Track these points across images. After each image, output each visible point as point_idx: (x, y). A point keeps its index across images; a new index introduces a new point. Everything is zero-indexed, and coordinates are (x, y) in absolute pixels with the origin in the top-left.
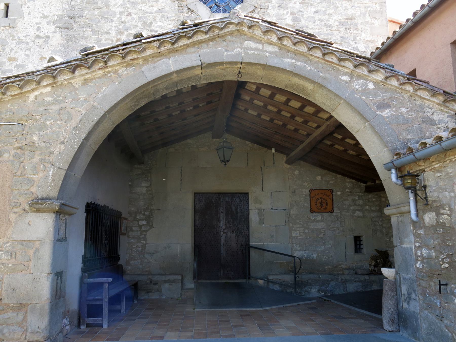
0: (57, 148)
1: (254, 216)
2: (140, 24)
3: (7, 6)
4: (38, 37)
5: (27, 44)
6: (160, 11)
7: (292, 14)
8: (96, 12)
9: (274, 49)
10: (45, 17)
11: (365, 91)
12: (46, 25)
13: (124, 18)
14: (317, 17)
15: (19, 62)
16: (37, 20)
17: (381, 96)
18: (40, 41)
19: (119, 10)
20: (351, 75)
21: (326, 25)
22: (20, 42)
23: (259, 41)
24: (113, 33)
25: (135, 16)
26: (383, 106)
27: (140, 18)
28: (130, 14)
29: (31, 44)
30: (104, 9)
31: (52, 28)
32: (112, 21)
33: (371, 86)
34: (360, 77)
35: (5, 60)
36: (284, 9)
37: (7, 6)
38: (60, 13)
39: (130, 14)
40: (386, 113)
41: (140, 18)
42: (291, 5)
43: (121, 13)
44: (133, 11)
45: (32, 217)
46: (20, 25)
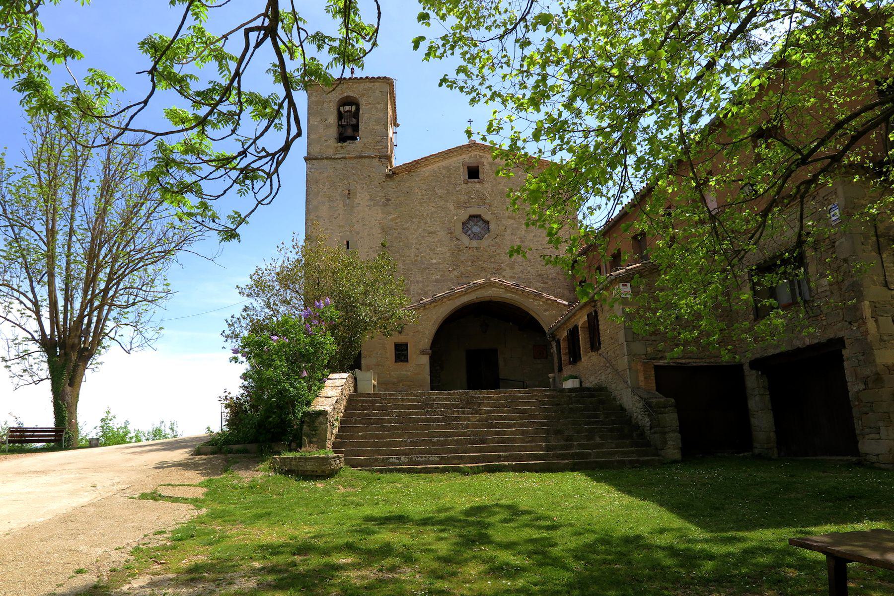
0: (427, 332)
1: (501, 362)
6: (439, 241)
7: (520, 238)
8: (401, 243)
9: (504, 290)
10: (371, 248)
11: (539, 305)
13: (418, 247)
14: (535, 239)
16: (366, 250)
17: (545, 307)
20: (533, 299)
21: (541, 244)
23: (498, 288)
24: (412, 256)
26: (546, 310)
27: (427, 246)
30: (406, 241)
33: (541, 303)
34: (537, 300)
36: (515, 235)
37: (348, 242)
40: (547, 313)
41: (427, 246)
42: (519, 232)
43: (416, 243)
45: (421, 356)
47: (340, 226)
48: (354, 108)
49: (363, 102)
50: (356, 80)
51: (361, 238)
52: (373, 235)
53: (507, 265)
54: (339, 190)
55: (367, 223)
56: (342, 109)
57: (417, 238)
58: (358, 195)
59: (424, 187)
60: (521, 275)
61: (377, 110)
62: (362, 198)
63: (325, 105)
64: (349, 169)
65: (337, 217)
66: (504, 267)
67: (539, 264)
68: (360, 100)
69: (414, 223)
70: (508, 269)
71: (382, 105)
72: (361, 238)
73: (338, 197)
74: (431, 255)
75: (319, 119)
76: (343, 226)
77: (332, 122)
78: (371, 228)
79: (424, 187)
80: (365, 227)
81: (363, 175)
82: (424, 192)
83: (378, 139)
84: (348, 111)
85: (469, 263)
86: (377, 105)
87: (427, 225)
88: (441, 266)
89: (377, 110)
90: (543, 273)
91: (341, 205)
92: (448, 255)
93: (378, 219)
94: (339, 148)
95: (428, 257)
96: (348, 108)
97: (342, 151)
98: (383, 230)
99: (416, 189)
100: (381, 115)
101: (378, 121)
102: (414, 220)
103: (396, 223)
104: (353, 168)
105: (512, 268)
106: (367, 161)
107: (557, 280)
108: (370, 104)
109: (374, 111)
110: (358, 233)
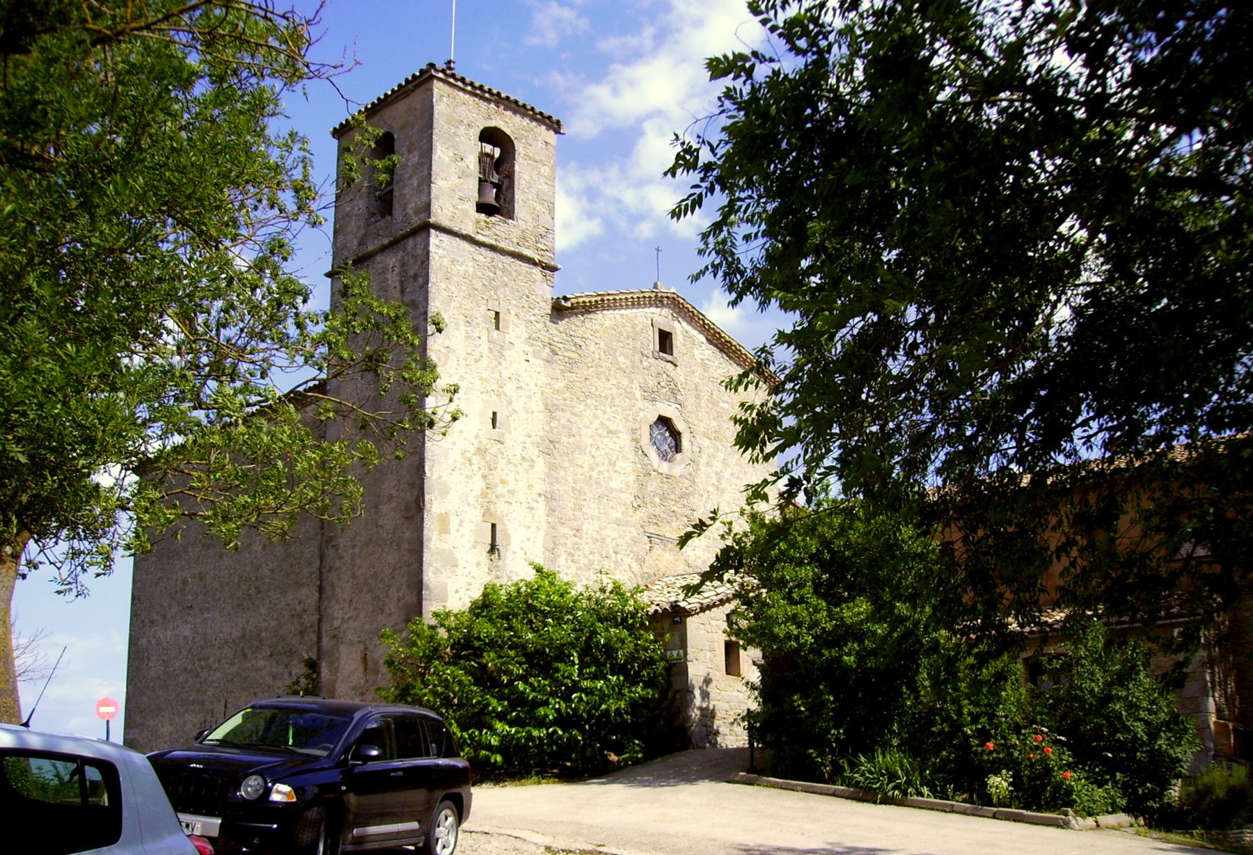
4: (523, 458)
5: (516, 466)
7: (717, 473)
12: (530, 447)
15: (511, 487)
16: (523, 438)
18: (526, 464)
19: (589, 441)
24: (586, 467)
28: (598, 448)
31: (536, 452)
32: (585, 454)
35: (497, 481)
37: (494, 414)
38: (541, 433)
39: (598, 448)
44: (600, 445)
46: (509, 439)
47: (481, 379)
50: (513, 106)
54: (483, 308)
55: (524, 386)
58: (511, 326)
61: (539, 173)
62: (515, 331)
64: (498, 272)
65: (476, 361)
71: (547, 168)
73: (480, 320)
74: (611, 472)
79: (602, 346)
80: (521, 392)
83: (542, 231)
85: (657, 500)
87: (606, 416)
88: (624, 496)
91: (485, 338)
92: (632, 478)
94: (482, 223)
95: (606, 475)
97: (486, 232)
98: (546, 405)
104: (504, 271)
106: (525, 267)
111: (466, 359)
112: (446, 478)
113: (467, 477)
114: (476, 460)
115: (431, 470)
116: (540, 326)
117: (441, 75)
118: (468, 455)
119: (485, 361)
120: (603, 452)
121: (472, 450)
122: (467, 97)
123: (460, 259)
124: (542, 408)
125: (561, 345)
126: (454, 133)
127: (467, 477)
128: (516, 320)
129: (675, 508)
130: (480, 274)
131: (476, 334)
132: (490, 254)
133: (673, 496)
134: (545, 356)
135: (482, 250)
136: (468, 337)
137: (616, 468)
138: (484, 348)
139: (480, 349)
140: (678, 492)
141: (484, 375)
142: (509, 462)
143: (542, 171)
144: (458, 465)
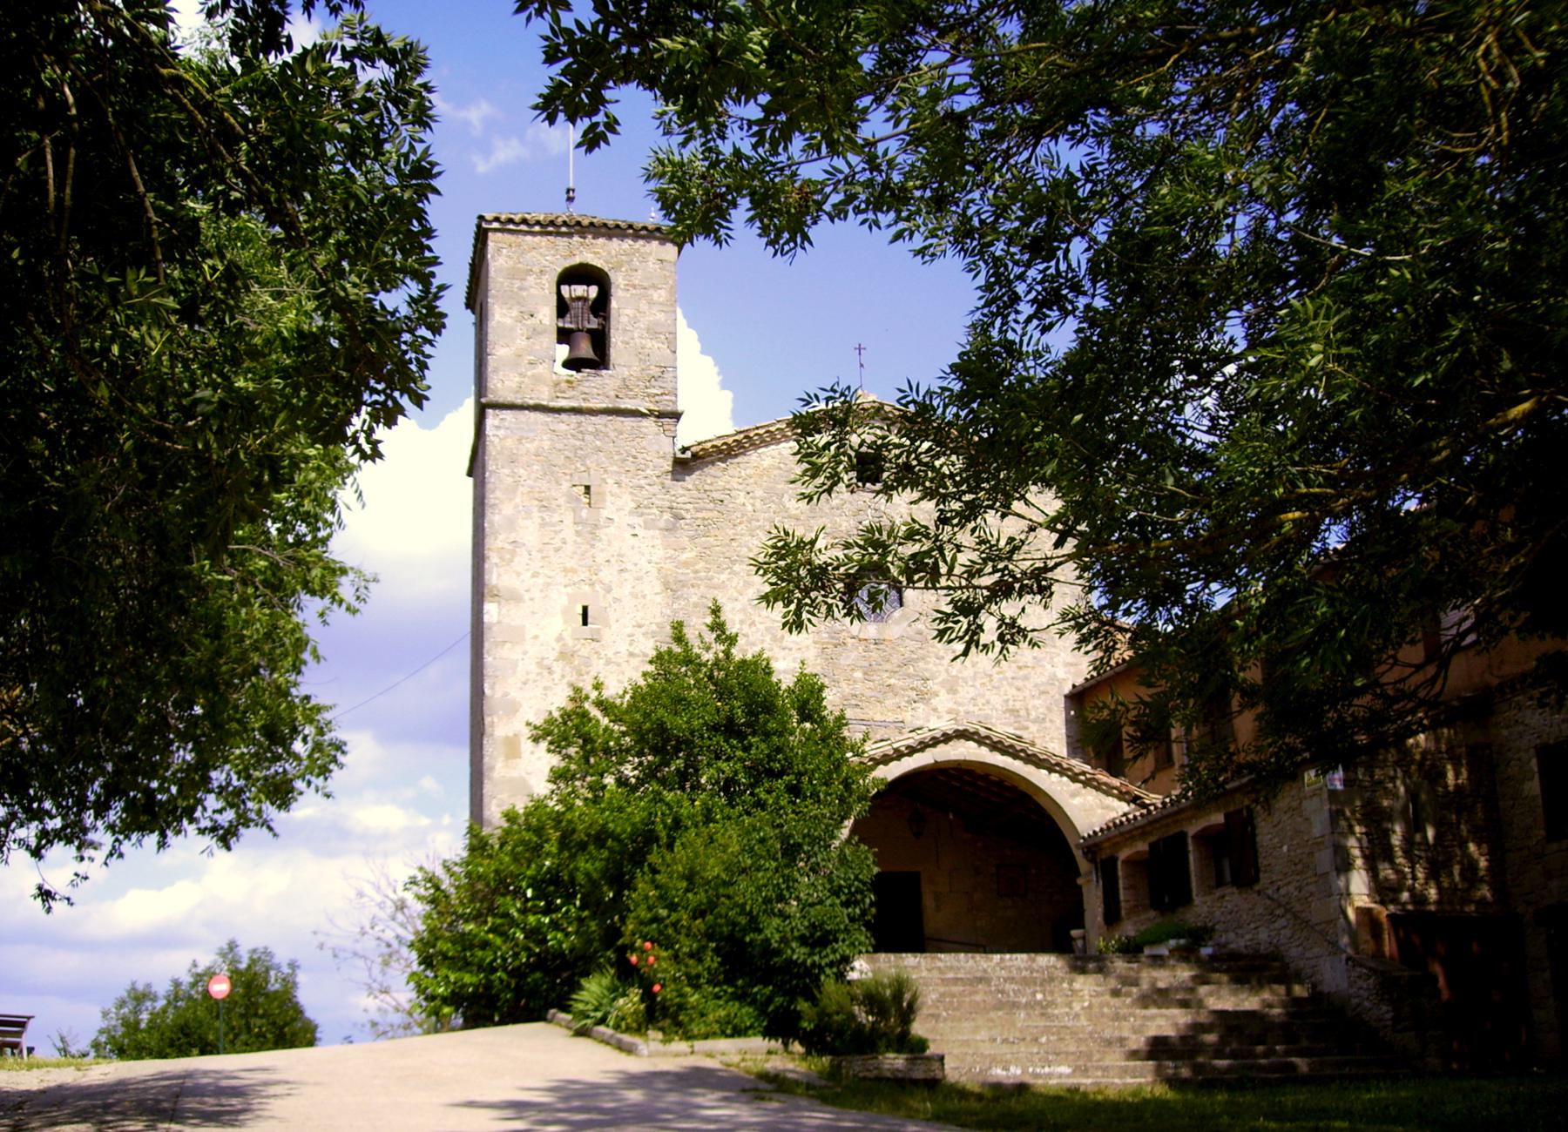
2: (768, 639)
3: (585, 609)
4: (631, 654)
5: (619, 665)
10: (640, 626)
12: (641, 638)
16: (629, 630)
22: (609, 662)
25: (762, 627)
26: (1074, 795)
28: (753, 624)
29: (624, 665)
37: (585, 609)
38: (659, 620)
39: (753, 624)
41: (767, 629)
43: (742, 622)
44: (757, 619)
46: (607, 635)
47: (565, 570)
48: (593, 292)
49: (618, 280)
51: (616, 600)
52: (644, 597)
53: (942, 684)
54: (566, 485)
55: (630, 566)
56: (565, 290)
57: (743, 610)
58: (609, 498)
59: (759, 493)
60: (971, 708)
61: (651, 303)
62: (617, 504)
63: (531, 279)
64: (587, 437)
65: (557, 550)
66: (936, 688)
67: (1011, 685)
68: (612, 275)
69: (736, 573)
70: (943, 693)
71: (663, 292)
72: (616, 600)
73: (562, 501)
75: (515, 313)
76: (573, 571)
77: (546, 321)
78: (639, 579)
79: (759, 493)
80: (625, 575)
81: (618, 453)
82: (758, 504)
83: (655, 371)
84: (579, 299)
85: (858, 674)
86: (651, 292)
89: (651, 303)
90: (1018, 705)
91: (569, 519)
93: (654, 559)
94: (564, 385)
96: (579, 290)
97: (570, 393)
98: (666, 586)
99: (742, 498)
100: (661, 317)
101: (653, 332)
102: (736, 568)
103: (696, 572)
104: (596, 434)
105: (952, 691)
106: (629, 422)
107: (1048, 724)
108: (634, 287)
109: (643, 306)
110: (609, 590)
111: (540, 551)
112: (514, 694)
113: (545, 688)
114: (557, 667)
115: (492, 688)
116: (656, 489)
117: (496, 225)
118: (546, 662)
119: (570, 547)
120: (762, 627)
121: (553, 655)
122: (538, 238)
123: (531, 435)
124: (658, 587)
125: (689, 506)
126: (521, 289)
127: (545, 688)
128: (615, 489)
129: (892, 681)
130: (560, 446)
131: (556, 518)
132: (574, 418)
133: (888, 666)
134: (662, 524)
135: (564, 416)
136: (543, 524)
137: (785, 644)
138: (569, 532)
139: (561, 536)
140: (896, 659)
141: (568, 565)
142: (609, 662)
143: (655, 297)
144: (532, 677)
